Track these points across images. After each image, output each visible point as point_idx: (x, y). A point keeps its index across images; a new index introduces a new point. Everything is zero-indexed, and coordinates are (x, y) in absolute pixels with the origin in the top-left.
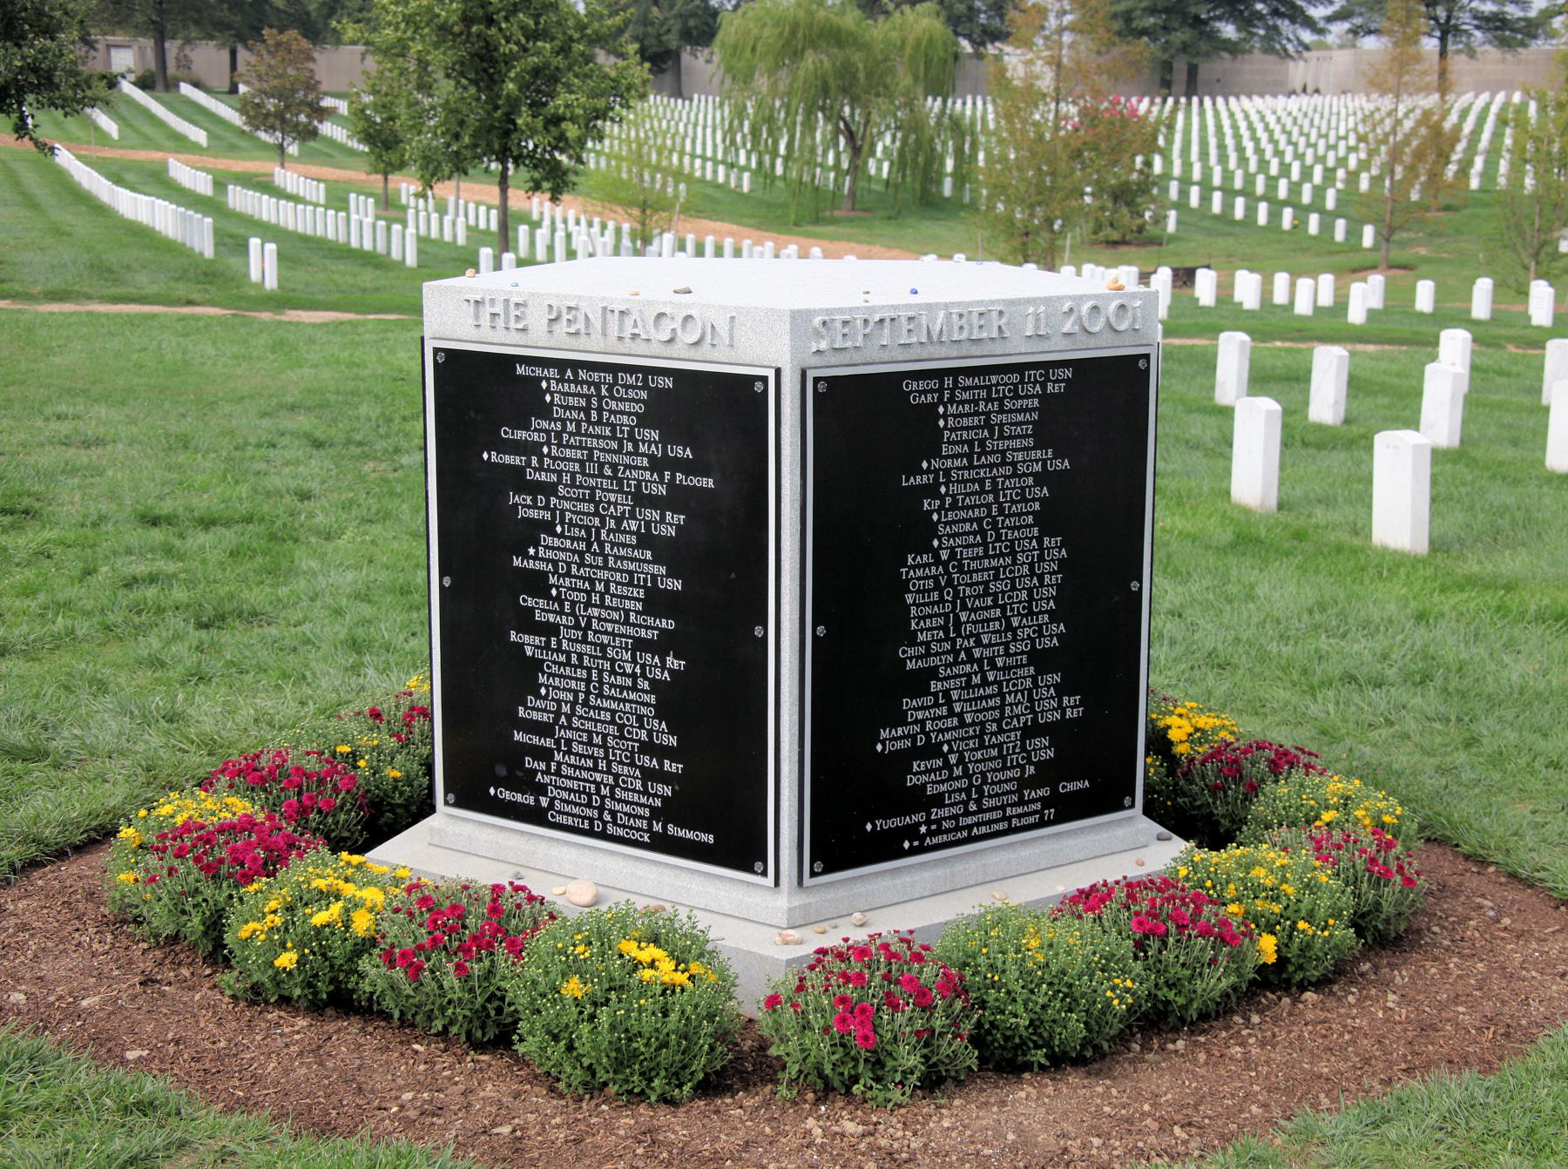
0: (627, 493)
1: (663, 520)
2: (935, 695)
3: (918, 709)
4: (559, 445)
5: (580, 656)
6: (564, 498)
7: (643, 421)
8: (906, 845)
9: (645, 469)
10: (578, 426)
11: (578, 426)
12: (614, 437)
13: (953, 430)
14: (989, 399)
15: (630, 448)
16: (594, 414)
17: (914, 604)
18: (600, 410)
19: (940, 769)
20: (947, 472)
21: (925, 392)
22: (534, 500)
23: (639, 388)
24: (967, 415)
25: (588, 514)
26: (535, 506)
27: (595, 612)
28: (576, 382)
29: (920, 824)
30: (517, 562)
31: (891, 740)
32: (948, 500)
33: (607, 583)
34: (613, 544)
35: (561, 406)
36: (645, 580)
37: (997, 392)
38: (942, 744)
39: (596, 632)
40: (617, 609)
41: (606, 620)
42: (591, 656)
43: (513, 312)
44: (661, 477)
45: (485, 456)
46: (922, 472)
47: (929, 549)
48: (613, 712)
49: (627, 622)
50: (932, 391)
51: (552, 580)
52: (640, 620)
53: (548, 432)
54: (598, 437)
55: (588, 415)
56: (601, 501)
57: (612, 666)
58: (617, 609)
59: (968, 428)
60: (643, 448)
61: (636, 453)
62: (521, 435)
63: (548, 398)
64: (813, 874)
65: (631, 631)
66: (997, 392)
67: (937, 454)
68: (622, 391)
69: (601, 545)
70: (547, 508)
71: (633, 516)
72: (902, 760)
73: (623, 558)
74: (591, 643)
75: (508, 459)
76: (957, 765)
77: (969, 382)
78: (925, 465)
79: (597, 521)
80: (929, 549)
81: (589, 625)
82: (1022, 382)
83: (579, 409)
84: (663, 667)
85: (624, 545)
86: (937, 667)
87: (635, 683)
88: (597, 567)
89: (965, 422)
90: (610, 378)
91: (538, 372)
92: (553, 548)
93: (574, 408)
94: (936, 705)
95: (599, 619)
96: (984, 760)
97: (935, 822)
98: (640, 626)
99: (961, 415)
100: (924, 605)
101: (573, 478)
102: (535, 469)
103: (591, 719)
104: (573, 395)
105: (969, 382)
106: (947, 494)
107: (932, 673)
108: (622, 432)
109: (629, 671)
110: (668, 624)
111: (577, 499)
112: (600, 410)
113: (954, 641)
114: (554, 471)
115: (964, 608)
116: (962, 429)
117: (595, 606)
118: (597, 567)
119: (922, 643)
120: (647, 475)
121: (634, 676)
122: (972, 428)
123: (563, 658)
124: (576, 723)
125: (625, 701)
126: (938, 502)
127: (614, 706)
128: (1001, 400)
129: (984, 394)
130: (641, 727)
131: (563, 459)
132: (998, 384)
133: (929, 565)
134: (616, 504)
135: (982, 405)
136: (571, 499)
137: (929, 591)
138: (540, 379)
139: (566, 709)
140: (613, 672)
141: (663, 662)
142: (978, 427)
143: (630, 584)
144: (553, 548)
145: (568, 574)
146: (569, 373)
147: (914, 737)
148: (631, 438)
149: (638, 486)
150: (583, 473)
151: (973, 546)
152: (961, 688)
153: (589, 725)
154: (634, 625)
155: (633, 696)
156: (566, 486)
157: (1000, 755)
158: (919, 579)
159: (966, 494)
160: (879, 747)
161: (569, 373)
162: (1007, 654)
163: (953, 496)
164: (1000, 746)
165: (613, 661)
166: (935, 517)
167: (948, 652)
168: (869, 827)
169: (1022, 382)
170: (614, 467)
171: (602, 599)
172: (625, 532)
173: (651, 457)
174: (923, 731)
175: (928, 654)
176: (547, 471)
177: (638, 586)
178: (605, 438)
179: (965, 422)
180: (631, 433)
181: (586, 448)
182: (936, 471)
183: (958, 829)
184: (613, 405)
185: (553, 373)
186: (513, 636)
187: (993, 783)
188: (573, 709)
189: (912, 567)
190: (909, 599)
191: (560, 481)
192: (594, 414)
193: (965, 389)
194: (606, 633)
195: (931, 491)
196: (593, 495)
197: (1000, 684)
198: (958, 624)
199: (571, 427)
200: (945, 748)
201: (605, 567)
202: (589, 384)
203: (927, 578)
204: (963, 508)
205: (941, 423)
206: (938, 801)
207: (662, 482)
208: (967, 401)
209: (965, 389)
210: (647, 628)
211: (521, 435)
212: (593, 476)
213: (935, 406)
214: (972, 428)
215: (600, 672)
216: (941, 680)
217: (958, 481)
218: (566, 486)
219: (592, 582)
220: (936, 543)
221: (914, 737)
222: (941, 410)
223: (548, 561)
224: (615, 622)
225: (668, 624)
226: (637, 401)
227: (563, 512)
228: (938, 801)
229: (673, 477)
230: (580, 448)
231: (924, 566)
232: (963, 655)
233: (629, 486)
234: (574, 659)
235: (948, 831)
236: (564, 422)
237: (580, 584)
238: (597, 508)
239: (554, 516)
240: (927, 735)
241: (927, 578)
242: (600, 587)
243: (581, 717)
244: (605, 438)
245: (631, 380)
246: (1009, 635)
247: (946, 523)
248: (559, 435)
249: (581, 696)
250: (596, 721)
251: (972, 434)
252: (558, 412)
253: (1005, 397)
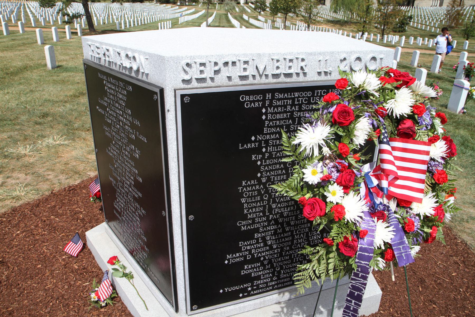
2: (257, 239)
3: (248, 245)
8: (241, 295)
13: (270, 121)
14: (293, 105)
17: (246, 202)
19: (259, 267)
20: (267, 142)
21: (254, 102)
24: (280, 113)
29: (248, 287)
31: (232, 258)
32: (267, 155)
37: (298, 101)
38: (260, 257)
46: (251, 142)
47: (255, 178)
50: (258, 101)
59: (280, 120)
64: (192, 310)
66: (298, 101)
67: (261, 132)
72: (240, 265)
76: (268, 265)
77: (281, 96)
78: (253, 138)
80: (255, 178)
82: (313, 96)
86: (259, 228)
89: (278, 116)
94: (258, 242)
96: (282, 261)
97: (255, 286)
99: (276, 113)
100: (252, 202)
105: (281, 96)
106: (266, 152)
107: (257, 230)
113: (268, 217)
115: (274, 202)
116: (276, 120)
119: (250, 219)
122: (282, 119)
126: (260, 156)
128: (300, 106)
129: (290, 102)
132: (299, 97)
133: (255, 185)
135: (289, 108)
137: (255, 196)
142: (285, 119)
147: (245, 257)
151: (280, 175)
152: (271, 235)
157: (290, 258)
158: (249, 191)
159: (277, 152)
160: (226, 262)
162: (297, 219)
163: (270, 153)
164: (290, 255)
166: (259, 163)
167: (265, 221)
168: (221, 291)
169: (313, 96)
174: (250, 253)
175: (254, 223)
179: (278, 116)
182: (260, 142)
183: (267, 286)
187: (286, 268)
189: (244, 186)
190: (243, 201)
193: (279, 100)
195: (258, 151)
197: (292, 232)
198: (271, 209)
200: (262, 259)
203: (254, 190)
204: (275, 158)
205: (264, 117)
206: (258, 278)
208: (279, 106)
209: (279, 100)
213: (260, 109)
214: (282, 119)
216: (261, 233)
217: (273, 146)
220: (259, 175)
221: (245, 257)
222: (264, 111)
228: (258, 278)
231: (252, 186)
232: (273, 222)
235: (261, 288)
240: (253, 255)
241: (254, 190)
246: (298, 212)
247: (265, 166)
251: (282, 123)
253: (302, 103)
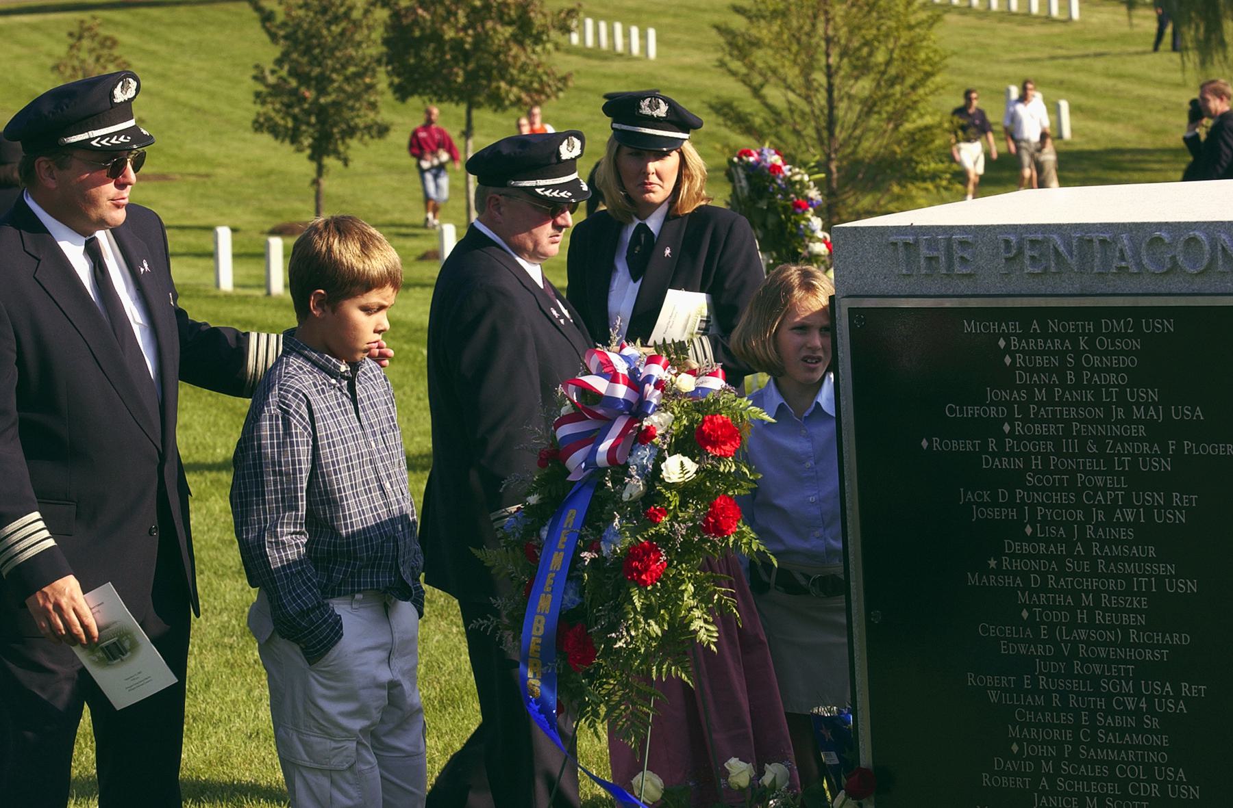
0: (1119, 474)
1: (1168, 504)
4: (1025, 420)
5: (1064, 696)
6: (1034, 488)
9: (1141, 440)
10: (1050, 393)
11: (1050, 393)
12: (1098, 403)
15: (1121, 414)
16: (1070, 376)
18: (1078, 370)
22: (994, 496)
23: (1130, 336)
25: (1067, 507)
26: (994, 503)
27: (1083, 634)
28: (1045, 335)
30: (973, 579)
33: (1097, 593)
34: (1103, 543)
35: (1026, 369)
36: (1149, 584)
39: (1084, 661)
40: (1111, 627)
41: (1097, 644)
42: (1078, 694)
43: (958, 252)
44: (1164, 448)
45: (925, 443)
48: (1112, 764)
49: (1126, 643)
51: (1023, 598)
52: (1144, 638)
53: (1009, 404)
54: (1077, 404)
55: (1062, 378)
56: (1084, 487)
57: (1109, 703)
58: (1111, 627)
60: (1138, 413)
61: (1129, 420)
62: (972, 411)
63: (1008, 360)
65: (1132, 654)
69: (1088, 548)
70: (1011, 504)
71: (1128, 503)
73: (1116, 559)
74: (1078, 677)
75: (955, 445)
79: (1080, 516)
81: (1074, 654)
83: (1050, 371)
84: (1177, 696)
85: (1118, 542)
87: (1140, 722)
88: (1083, 575)
90: (1090, 327)
91: (994, 327)
92: (1022, 556)
93: (1042, 370)
95: (1088, 643)
98: (1145, 646)
101: (1046, 461)
102: (994, 455)
103: (1082, 778)
108: (1109, 395)
109: (1131, 707)
110: (1180, 639)
111: (1053, 489)
112: (1078, 370)
114: (1018, 455)
117: (1082, 626)
118: (1083, 575)
120: (1146, 448)
121: (1138, 712)
123: (1040, 701)
124: (1062, 785)
125: (1127, 747)
127: (1113, 755)
130: (1152, 779)
131: (1030, 439)
134: (1104, 489)
136: (1044, 489)
139: (1047, 767)
140: (1109, 711)
141: (1177, 690)
143: (1129, 592)
144: (1022, 556)
145: (1044, 588)
146: (1035, 325)
148: (1122, 402)
149: (1134, 463)
150: (1058, 452)
153: (1079, 786)
154: (1135, 646)
155: (1138, 740)
156: (1036, 472)
161: (1035, 325)
165: (1109, 696)
170: (1100, 441)
171: (1091, 617)
172: (1119, 524)
173: (1149, 424)
176: (1011, 454)
177: (1140, 594)
178: (1087, 404)
180: (1121, 394)
181: (1062, 420)
184: (1096, 361)
185: (1013, 327)
186: (971, 680)
188: (1057, 768)
191: (1027, 463)
192: (1070, 376)
194: (1098, 660)
196: (1072, 481)
199: (1041, 395)
201: (1094, 573)
207: (1164, 454)
210: (1153, 647)
211: (972, 411)
212: (1072, 456)
215: (1092, 713)
218: (1036, 472)
219: (1076, 595)
223: (1015, 574)
224: (1112, 644)
225: (1180, 639)
226: (1127, 354)
227: (1033, 507)
229: (1180, 446)
230: (1054, 420)
233: (1121, 464)
234: (1056, 701)
236: (1030, 389)
237: (1060, 599)
238: (1079, 496)
239: (1021, 513)
242: (1088, 600)
243: (1068, 777)
244: (1087, 404)
245: (1118, 326)
248: (1024, 408)
249: (1068, 749)
250: (1088, 779)
252: (1021, 377)
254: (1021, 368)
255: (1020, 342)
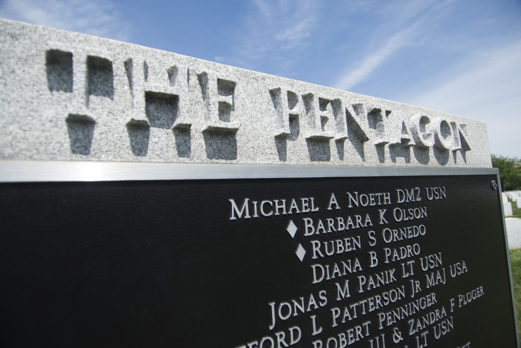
7: (427, 245)
55: (366, 262)
63: (301, 253)
68: (403, 212)
91: (280, 206)
93: (345, 256)
104: (341, 235)
138: (284, 220)
146: (333, 200)
161: (333, 200)
180: (417, 266)
184: (395, 235)
185: (308, 205)
202: (362, 211)
236: (329, 286)
248: (324, 315)
254: (320, 260)
255: (315, 225)
